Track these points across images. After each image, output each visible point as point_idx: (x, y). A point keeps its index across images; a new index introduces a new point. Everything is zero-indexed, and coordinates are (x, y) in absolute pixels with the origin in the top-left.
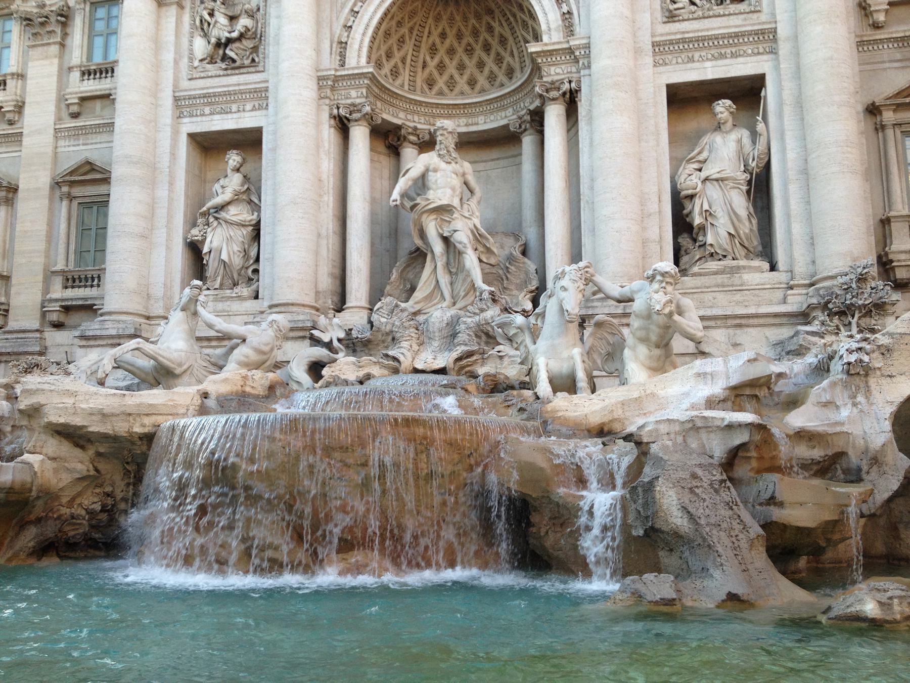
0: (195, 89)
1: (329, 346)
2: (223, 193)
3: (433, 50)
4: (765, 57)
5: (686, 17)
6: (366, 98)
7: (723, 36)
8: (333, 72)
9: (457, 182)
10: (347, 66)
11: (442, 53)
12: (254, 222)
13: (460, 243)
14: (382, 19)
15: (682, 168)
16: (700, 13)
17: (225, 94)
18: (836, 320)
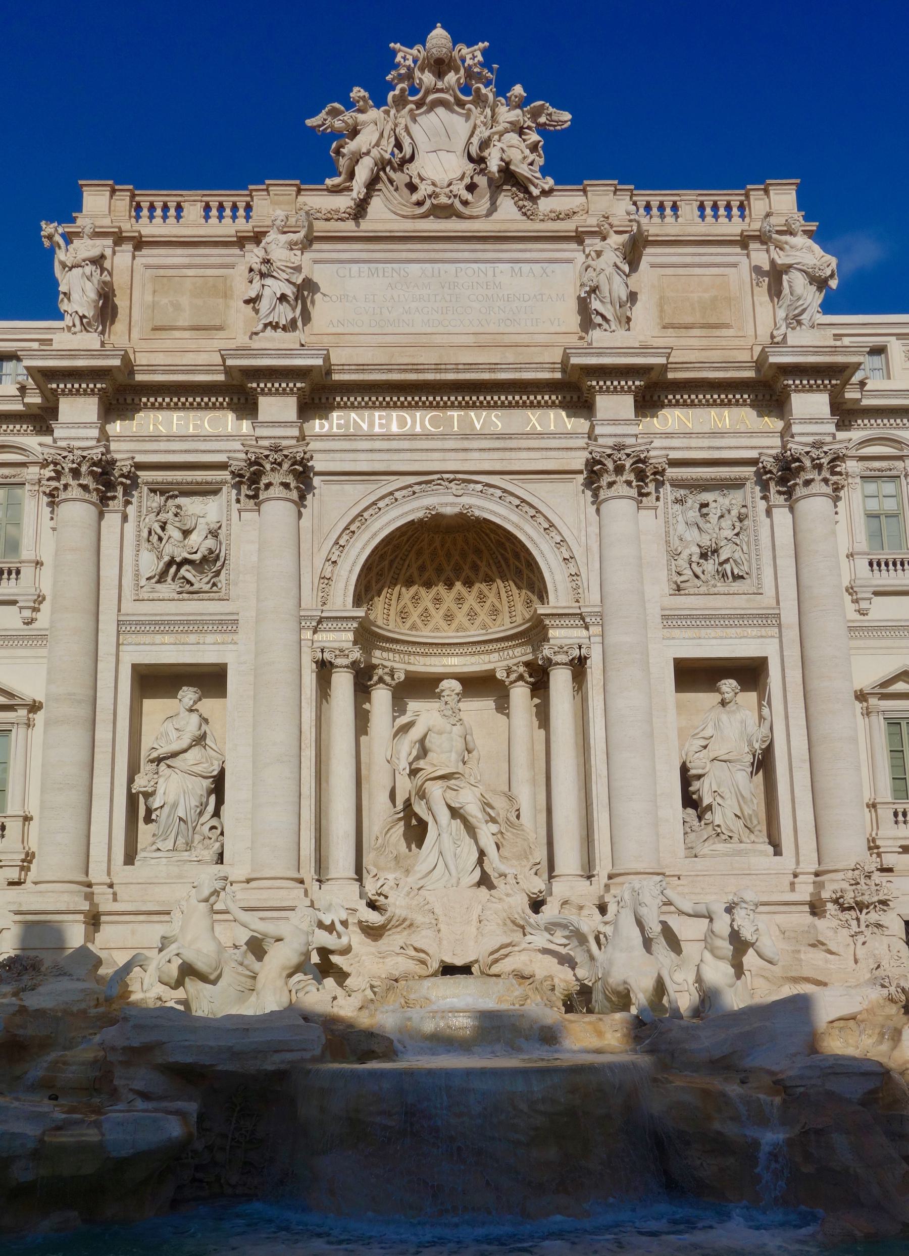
1: (330, 928)
5: (692, 591)
6: (355, 643)
7: (730, 617)
8: (319, 614)
9: (459, 744)
12: (215, 773)
14: (370, 556)
15: (687, 744)
16: (703, 589)
17: (181, 622)
18: (847, 915)
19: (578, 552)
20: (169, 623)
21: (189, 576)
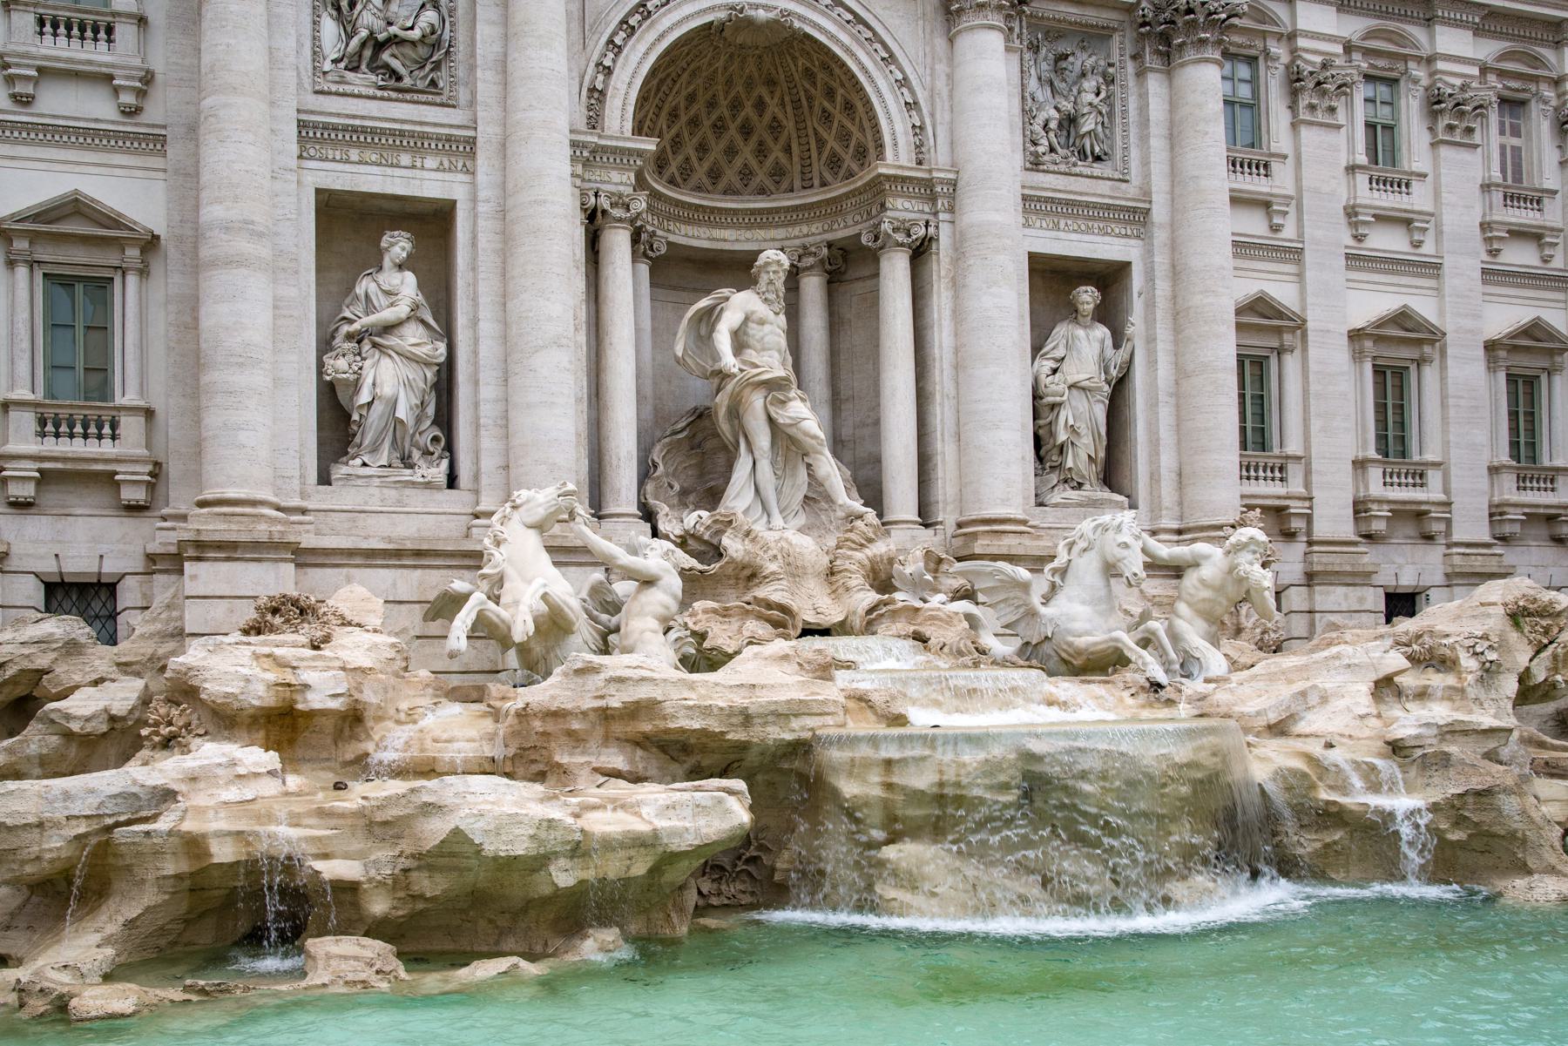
0: (338, 115)
2: (392, 305)
3: (674, 115)
4: (1133, 242)
5: (1052, 167)
7: (1095, 206)
8: (595, 139)
10: (607, 132)
11: (684, 119)
12: (442, 359)
13: (815, 437)
16: (1063, 168)
17: (392, 133)
19: (922, 97)
20: (373, 131)
21: (396, 64)
